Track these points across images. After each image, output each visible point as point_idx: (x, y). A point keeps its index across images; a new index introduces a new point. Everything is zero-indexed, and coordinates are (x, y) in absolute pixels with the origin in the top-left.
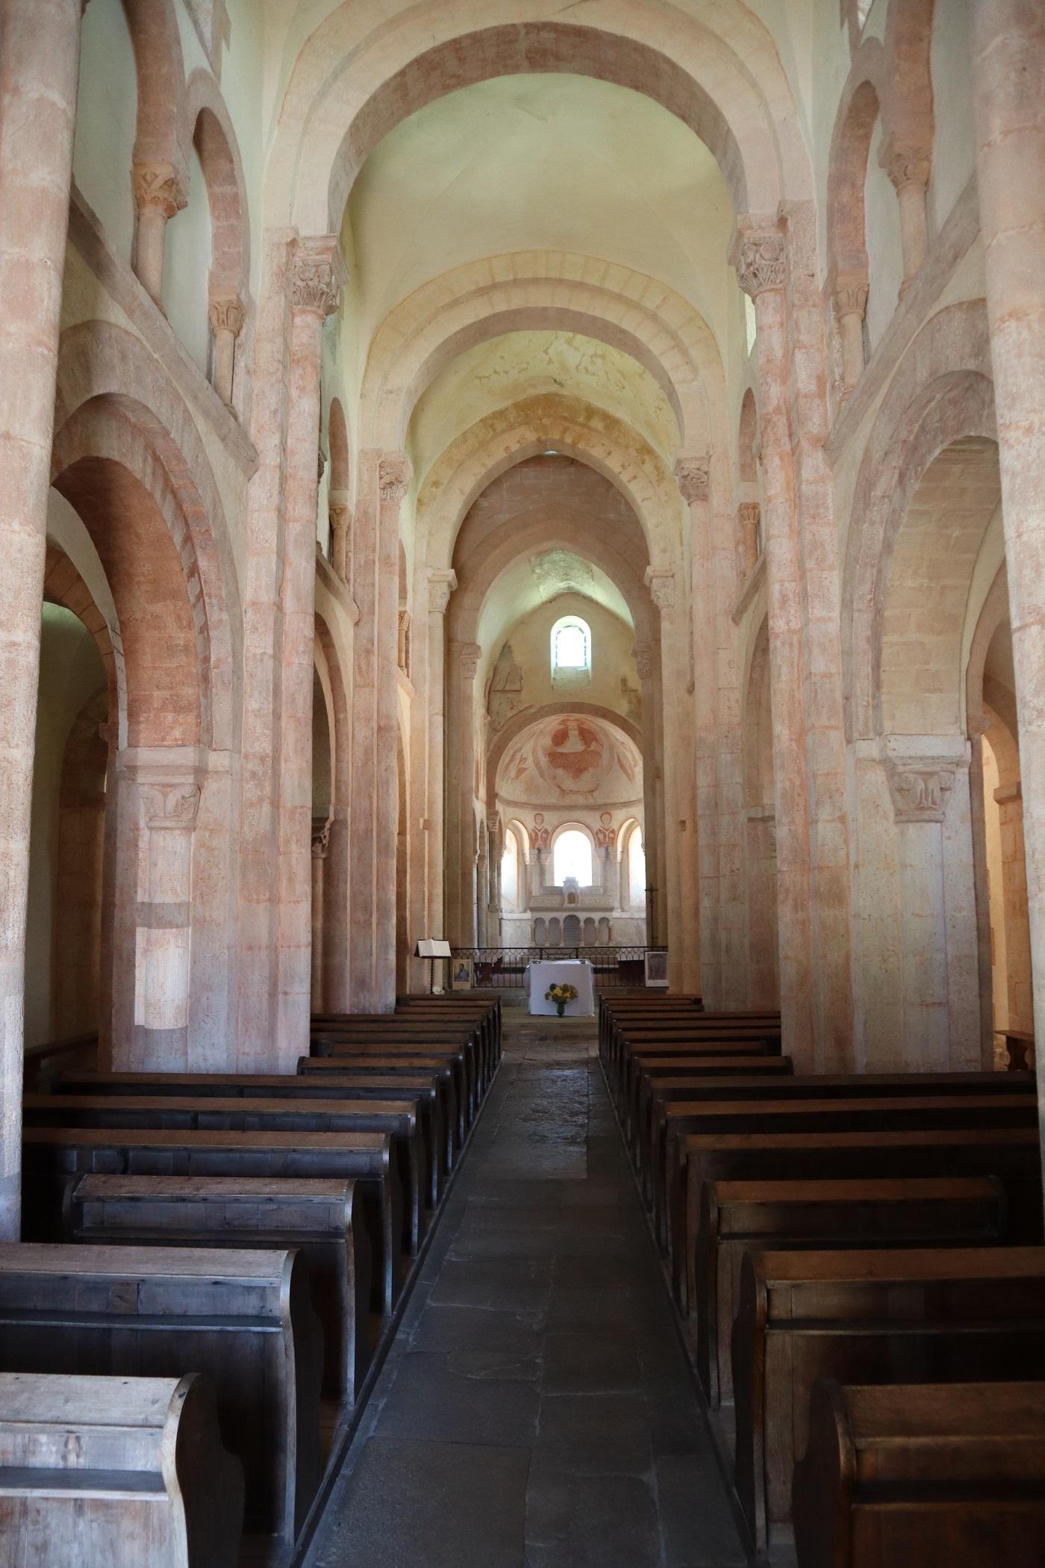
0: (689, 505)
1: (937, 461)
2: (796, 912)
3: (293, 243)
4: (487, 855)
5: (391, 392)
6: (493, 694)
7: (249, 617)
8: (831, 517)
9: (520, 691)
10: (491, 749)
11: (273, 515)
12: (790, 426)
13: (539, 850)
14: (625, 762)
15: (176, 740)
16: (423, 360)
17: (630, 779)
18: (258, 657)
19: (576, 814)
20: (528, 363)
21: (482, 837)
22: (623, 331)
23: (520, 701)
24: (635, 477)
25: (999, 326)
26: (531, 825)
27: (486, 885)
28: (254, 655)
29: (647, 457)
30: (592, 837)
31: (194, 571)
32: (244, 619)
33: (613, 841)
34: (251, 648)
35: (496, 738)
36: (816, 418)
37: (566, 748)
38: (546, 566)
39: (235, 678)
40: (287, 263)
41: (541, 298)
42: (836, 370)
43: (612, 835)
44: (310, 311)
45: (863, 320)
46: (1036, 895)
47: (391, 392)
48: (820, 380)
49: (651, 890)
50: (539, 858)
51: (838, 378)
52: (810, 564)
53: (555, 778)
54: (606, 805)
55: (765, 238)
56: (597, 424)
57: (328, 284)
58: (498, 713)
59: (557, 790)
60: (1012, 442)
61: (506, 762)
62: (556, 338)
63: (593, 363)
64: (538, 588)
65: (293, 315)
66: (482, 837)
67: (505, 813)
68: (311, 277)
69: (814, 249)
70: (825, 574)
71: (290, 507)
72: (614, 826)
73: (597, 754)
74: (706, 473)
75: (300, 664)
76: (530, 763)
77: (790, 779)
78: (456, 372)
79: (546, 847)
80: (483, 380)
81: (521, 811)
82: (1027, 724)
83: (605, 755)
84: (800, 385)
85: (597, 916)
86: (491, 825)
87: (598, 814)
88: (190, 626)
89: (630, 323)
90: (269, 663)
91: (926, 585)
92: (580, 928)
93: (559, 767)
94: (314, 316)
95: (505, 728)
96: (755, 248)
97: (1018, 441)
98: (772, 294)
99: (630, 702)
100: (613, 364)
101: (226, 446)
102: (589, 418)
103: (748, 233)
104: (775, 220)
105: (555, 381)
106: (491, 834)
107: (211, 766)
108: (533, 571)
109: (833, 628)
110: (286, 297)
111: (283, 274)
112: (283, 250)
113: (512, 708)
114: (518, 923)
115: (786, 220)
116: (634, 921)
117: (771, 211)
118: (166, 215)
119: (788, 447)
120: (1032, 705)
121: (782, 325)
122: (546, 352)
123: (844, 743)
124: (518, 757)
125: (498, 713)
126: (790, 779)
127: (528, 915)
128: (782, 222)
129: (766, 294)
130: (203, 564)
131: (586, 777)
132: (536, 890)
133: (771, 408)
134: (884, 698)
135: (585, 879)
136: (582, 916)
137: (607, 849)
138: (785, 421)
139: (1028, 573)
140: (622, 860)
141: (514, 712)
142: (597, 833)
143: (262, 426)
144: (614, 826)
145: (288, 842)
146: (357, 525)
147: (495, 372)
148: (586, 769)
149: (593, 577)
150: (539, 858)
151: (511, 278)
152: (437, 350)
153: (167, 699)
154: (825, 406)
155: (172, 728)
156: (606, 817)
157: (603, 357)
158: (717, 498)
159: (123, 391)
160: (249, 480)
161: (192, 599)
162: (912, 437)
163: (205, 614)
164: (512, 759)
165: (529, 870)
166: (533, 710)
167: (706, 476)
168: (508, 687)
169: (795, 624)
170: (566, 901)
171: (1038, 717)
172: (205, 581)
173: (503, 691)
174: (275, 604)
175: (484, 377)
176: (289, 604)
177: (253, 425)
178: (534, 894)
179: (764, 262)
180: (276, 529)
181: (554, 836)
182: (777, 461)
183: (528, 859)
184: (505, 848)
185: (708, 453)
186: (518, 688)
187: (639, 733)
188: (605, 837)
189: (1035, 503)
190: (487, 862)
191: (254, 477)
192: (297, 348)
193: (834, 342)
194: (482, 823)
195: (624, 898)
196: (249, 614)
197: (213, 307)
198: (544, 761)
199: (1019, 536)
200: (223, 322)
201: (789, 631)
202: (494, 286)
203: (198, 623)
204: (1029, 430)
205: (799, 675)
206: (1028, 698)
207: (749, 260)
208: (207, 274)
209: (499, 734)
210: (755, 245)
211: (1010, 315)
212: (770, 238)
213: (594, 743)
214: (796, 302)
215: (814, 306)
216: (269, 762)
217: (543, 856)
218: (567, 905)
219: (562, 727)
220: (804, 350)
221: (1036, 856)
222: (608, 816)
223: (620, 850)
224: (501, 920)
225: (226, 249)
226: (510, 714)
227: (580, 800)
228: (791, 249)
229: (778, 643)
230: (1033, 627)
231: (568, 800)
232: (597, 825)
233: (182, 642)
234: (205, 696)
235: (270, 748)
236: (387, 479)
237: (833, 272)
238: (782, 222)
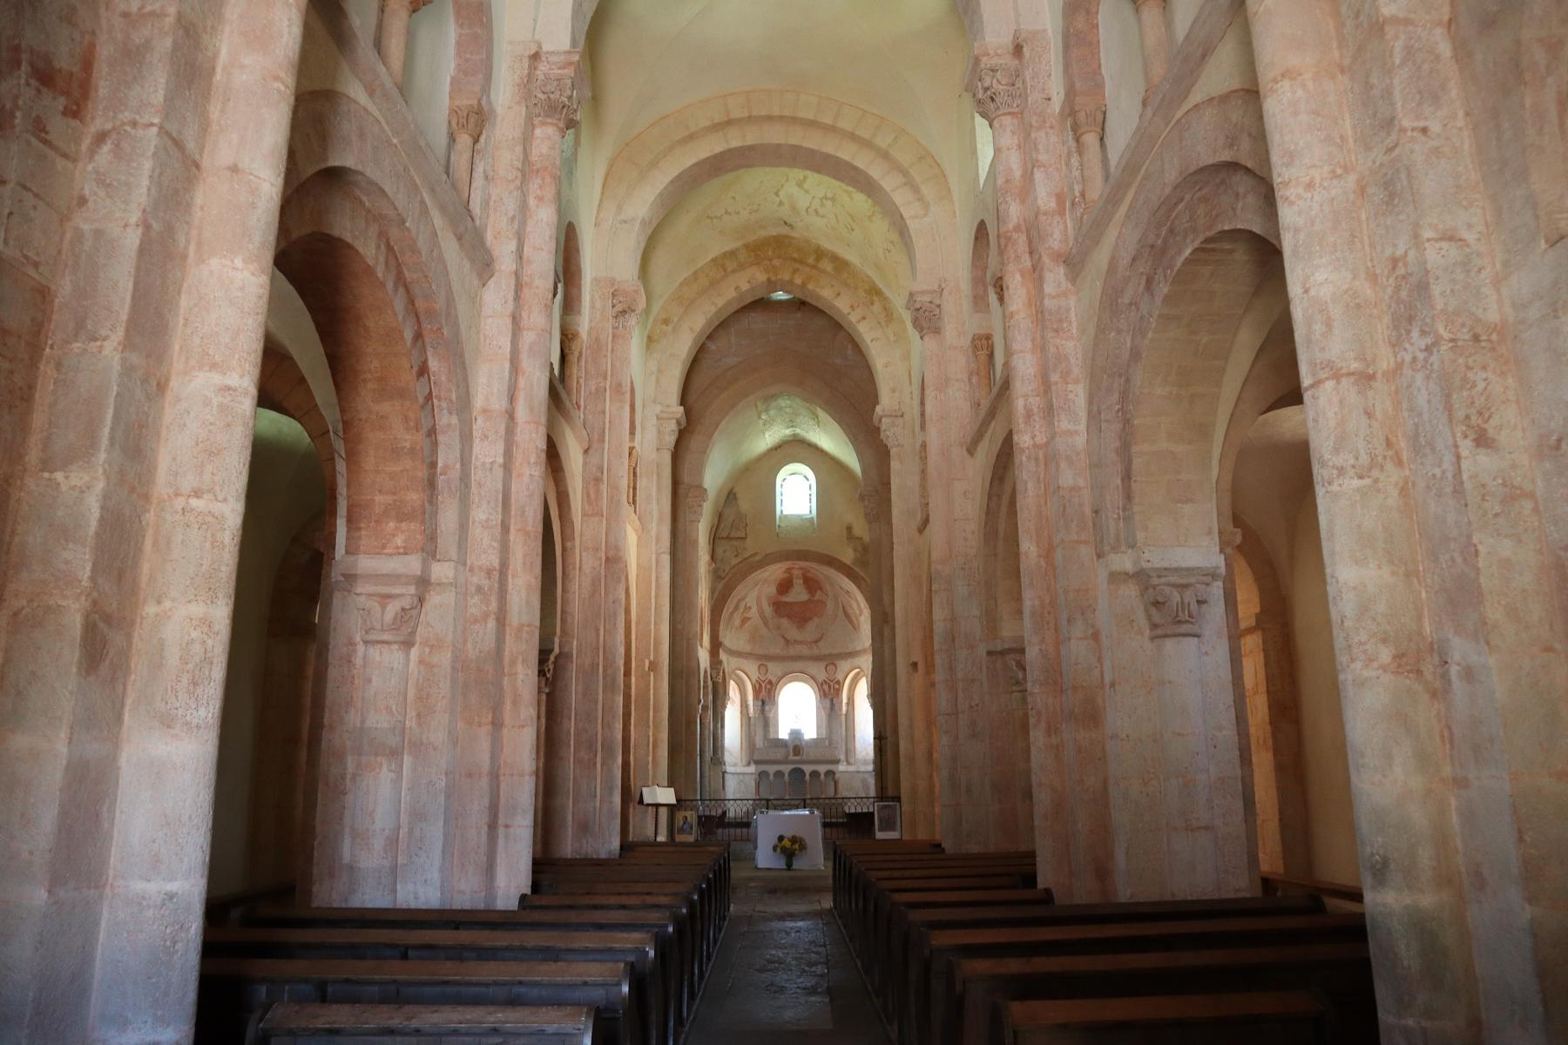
0: (922, 338)
1: (1188, 261)
2: (1049, 736)
3: (535, 57)
4: (710, 705)
5: (625, 222)
6: (717, 540)
7: (479, 425)
8: (1074, 331)
10: (716, 595)
11: (508, 321)
12: (1030, 242)
14: (850, 611)
15: (397, 548)
16: (658, 191)
17: (855, 629)
18: (488, 466)
19: (800, 665)
20: (759, 205)
21: (705, 687)
22: (855, 169)
24: (864, 318)
25: (1271, 88)
26: (755, 676)
27: (709, 737)
28: (484, 464)
29: (875, 298)
30: (817, 689)
31: (423, 371)
32: (474, 427)
33: (838, 692)
34: (480, 457)
35: (720, 586)
36: (1057, 235)
37: (790, 598)
38: (772, 412)
39: (462, 485)
40: (529, 75)
41: (774, 135)
42: (1076, 187)
43: (837, 686)
44: (551, 124)
45: (1102, 139)
46: (1348, 666)
47: (625, 222)
48: (1060, 198)
49: (879, 738)
50: (763, 711)
51: (1078, 194)
52: (1055, 378)
53: (779, 628)
54: (830, 655)
55: (1001, 64)
56: (826, 265)
57: (570, 98)
58: (722, 560)
59: (783, 640)
60: (1293, 198)
61: (730, 610)
62: (787, 180)
63: (822, 205)
64: (764, 434)
65: (534, 127)
66: (705, 687)
67: (728, 663)
68: (553, 90)
69: (1050, 75)
70: (1070, 387)
71: (525, 315)
72: (840, 677)
73: (822, 603)
74: (939, 306)
75: (531, 475)
76: (754, 611)
77: (1040, 597)
78: (688, 211)
79: (770, 699)
80: (715, 221)
81: (745, 661)
82: (1326, 484)
83: (830, 604)
84: (1040, 202)
85: (822, 769)
86: (714, 675)
87: (822, 665)
88: (417, 428)
89: (862, 160)
90: (499, 473)
91: (1175, 392)
92: (805, 782)
93: (783, 617)
94: (555, 129)
95: (730, 575)
96: (991, 73)
97: (1299, 197)
98: (1009, 118)
99: (855, 550)
100: (843, 206)
101: (461, 246)
102: (818, 259)
103: (984, 59)
104: (1011, 47)
105: (786, 223)
106: (715, 684)
107: (434, 578)
108: (760, 418)
109: (1080, 441)
110: (527, 107)
111: (527, 85)
112: (526, 64)
113: (736, 556)
114: (741, 777)
115: (1022, 47)
116: (861, 775)
117: (1007, 40)
118: (411, 9)
119: (1028, 264)
120: (1331, 464)
121: (1020, 147)
122: (777, 194)
123: (1095, 558)
125: (722, 560)
126: (1040, 597)
127: (752, 769)
128: (1018, 50)
129: (1003, 118)
130: (433, 364)
131: (811, 626)
132: (759, 743)
133: (1011, 226)
134: (1136, 509)
135: (810, 732)
136: (807, 769)
137: (832, 701)
138: (1025, 238)
139: (1318, 328)
141: (739, 560)
142: (822, 685)
143: (499, 233)
144: (840, 677)
145: (513, 663)
146: (589, 351)
147: (727, 212)
148: (810, 619)
149: (818, 422)
150: (763, 711)
151: (747, 115)
152: (672, 182)
153: (390, 505)
154: (1065, 223)
155: (394, 535)
157: (833, 199)
158: (950, 331)
159: (360, 168)
160: (484, 285)
161: (421, 400)
162: (1160, 242)
163: (434, 416)
164: (737, 608)
166: (757, 558)
167: (938, 310)
168: (732, 535)
169: (1041, 439)
170: (791, 754)
171: (1338, 477)
172: (434, 383)
173: (728, 538)
174: (506, 411)
175: (716, 217)
176: (522, 413)
177: (489, 230)
178: (757, 747)
179: (1001, 87)
180: (510, 335)
181: (778, 687)
182: (1018, 277)
184: (729, 700)
185: (940, 286)
186: (743, 535)
187: (865, 581)
188: (830, 687)
189: (1321, 257)
190: (710, 712)
191: (489, 282)
192: (537, 159)
193: (1073, 160)
194: (706, 672)
195: (850, 750)
196: (479, 421)
197: (454, 111)
198: (768, 610)
199: (1306, 291)
200: (463, 125)
201: (1035, 445)
202: (729, 123)
203: (426, 425)
204: (1310, 186)
205: (1045, 490)
206: (1327, 456)
207: (986, 85)
208: (449, 79)
209: (724, 581)
210: (992, 70)
211: (1283, 75)
212: (1006, 64)
213: (819, 592)
214: (1034, 124)
215: (1051, 127)
216: (496, 575)
217: (767, 708)
218: (791, 757)
219: (786, 575)
220: (1042, 169)
221: (1345, 624)
222: (832, 666)
223: (845, 700)
224: (724, 773)
225: (468, 56)
226: (735, 561)
227: (805, 651)
228: (1028, 74)
229: (1024, 459)
230: (1327, 383)
231: (794, 650)
232: (822, 676)
233: (408, 445)
234: (431, 502)
235: (498, 561)
236: (619, 308)
237: (1071, 93)
238: (1018, 50)
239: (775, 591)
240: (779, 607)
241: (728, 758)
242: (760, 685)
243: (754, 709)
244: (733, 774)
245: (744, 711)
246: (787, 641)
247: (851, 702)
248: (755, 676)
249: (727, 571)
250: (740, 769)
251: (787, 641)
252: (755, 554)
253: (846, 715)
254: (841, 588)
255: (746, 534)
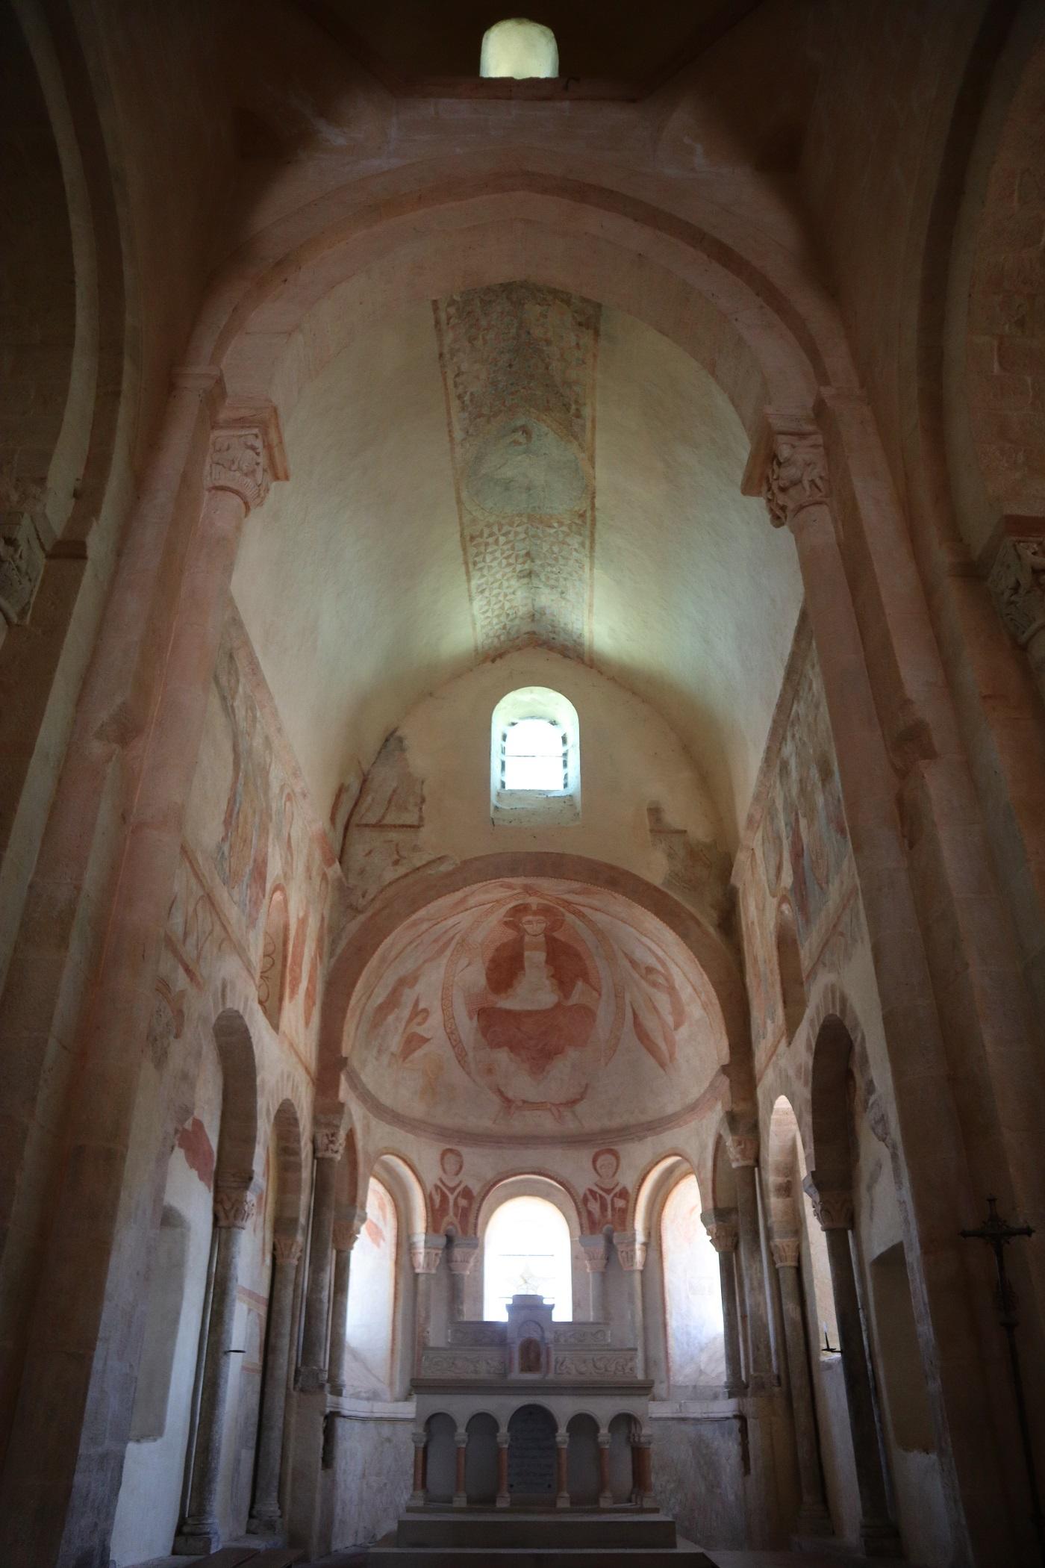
6: (354, 832)
9: (418, 827)
10: (339, 951)
13: (450, 1241)
14: (650, 1023)
17: (662, 1065)
19: (533, 1156)
23: (415, 848)
26: (433, 1175)
30: (574, 1214)
33: (624, 1216)
35: (353, 926)
37: (518, 1000)
43: (620, 1203)
50: (448, 1260)
53: (490, 1071)
54: (605, 1132)
58: (362, 872)
59: (496, 1098)
67: (367, 1128)
72: (627, 1180)
73: (587, 1013)
76: (433, 1026)
79: (465, 1232)
81: (411, 1136)
83: (604, 1014)
85: (604, 1409)
86: (322, 1141)
87: (585, 1156)
92: (554, 1448)
93: (499, 1045)
95: (378, 905)
99: (671, 856)
113: (396, 863)
114: (386, 1430)
116: (688, 1428)
124: (408, 996)
125: (362, 872)
127: (408, 1409)
131: (561, 1068)
132: (437, 1334)
136: (564, 1408)
137: (609, 1240)
140: (645, 1264)
141: (401, 870)
142: (585, 1200)
144: (627, 1180)
148: (559, 1051)
150: (448, 1260)
156: (605, 1160)
164: (392, 1002)
165: (422, 1287)
166: (444, 868)
168: (389, 820)
173: (379, 826)
183: (421, 1258)
186: (410, 818)
187: (698, 923)
188: (603, 1207)
198: (467, 1027)
209: (361, 918)
213: (580, 984)
217: (458, 1253)
218: (516, 1375)
219: (510, 934)
222: (610, 1158)
223: (640, 1238)
224: (331, 1418)
226: (390, 875)
231: (522, 1123)
232: (585, 1180)
239: (483, 981)
240: (489, 1018)
241: (350, 1374)
242: (444, 1198)
243: (427, 1254)
244: (364, 1420)
245: (405, 1259)
246: (508, 1102)
247: (653, 1243)
248: (433, 1175)
249: (369, 897)
250: (384, 1408)
251: (508, 1102)
252: (441, 859)
253: (642, 1272)
254: (634, 963)
255: (421, 818)
